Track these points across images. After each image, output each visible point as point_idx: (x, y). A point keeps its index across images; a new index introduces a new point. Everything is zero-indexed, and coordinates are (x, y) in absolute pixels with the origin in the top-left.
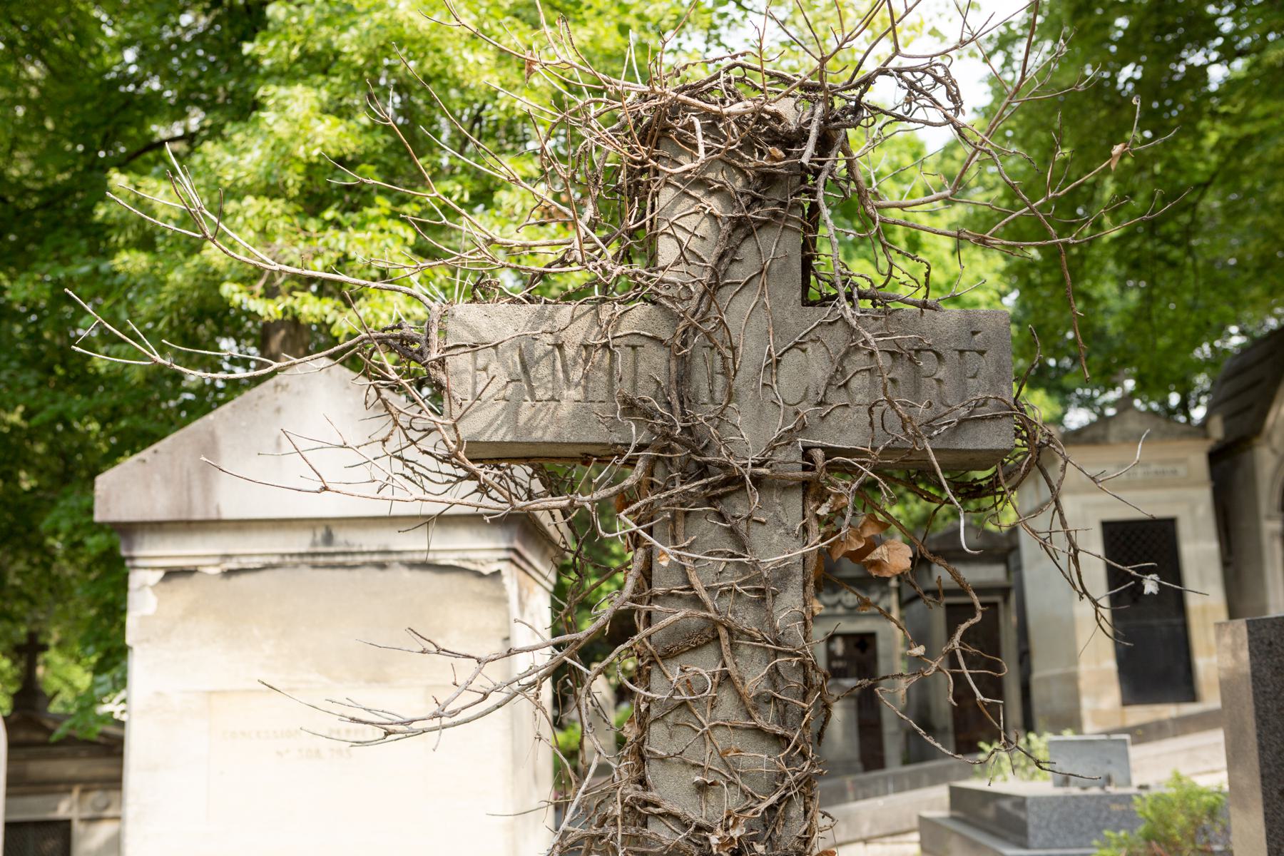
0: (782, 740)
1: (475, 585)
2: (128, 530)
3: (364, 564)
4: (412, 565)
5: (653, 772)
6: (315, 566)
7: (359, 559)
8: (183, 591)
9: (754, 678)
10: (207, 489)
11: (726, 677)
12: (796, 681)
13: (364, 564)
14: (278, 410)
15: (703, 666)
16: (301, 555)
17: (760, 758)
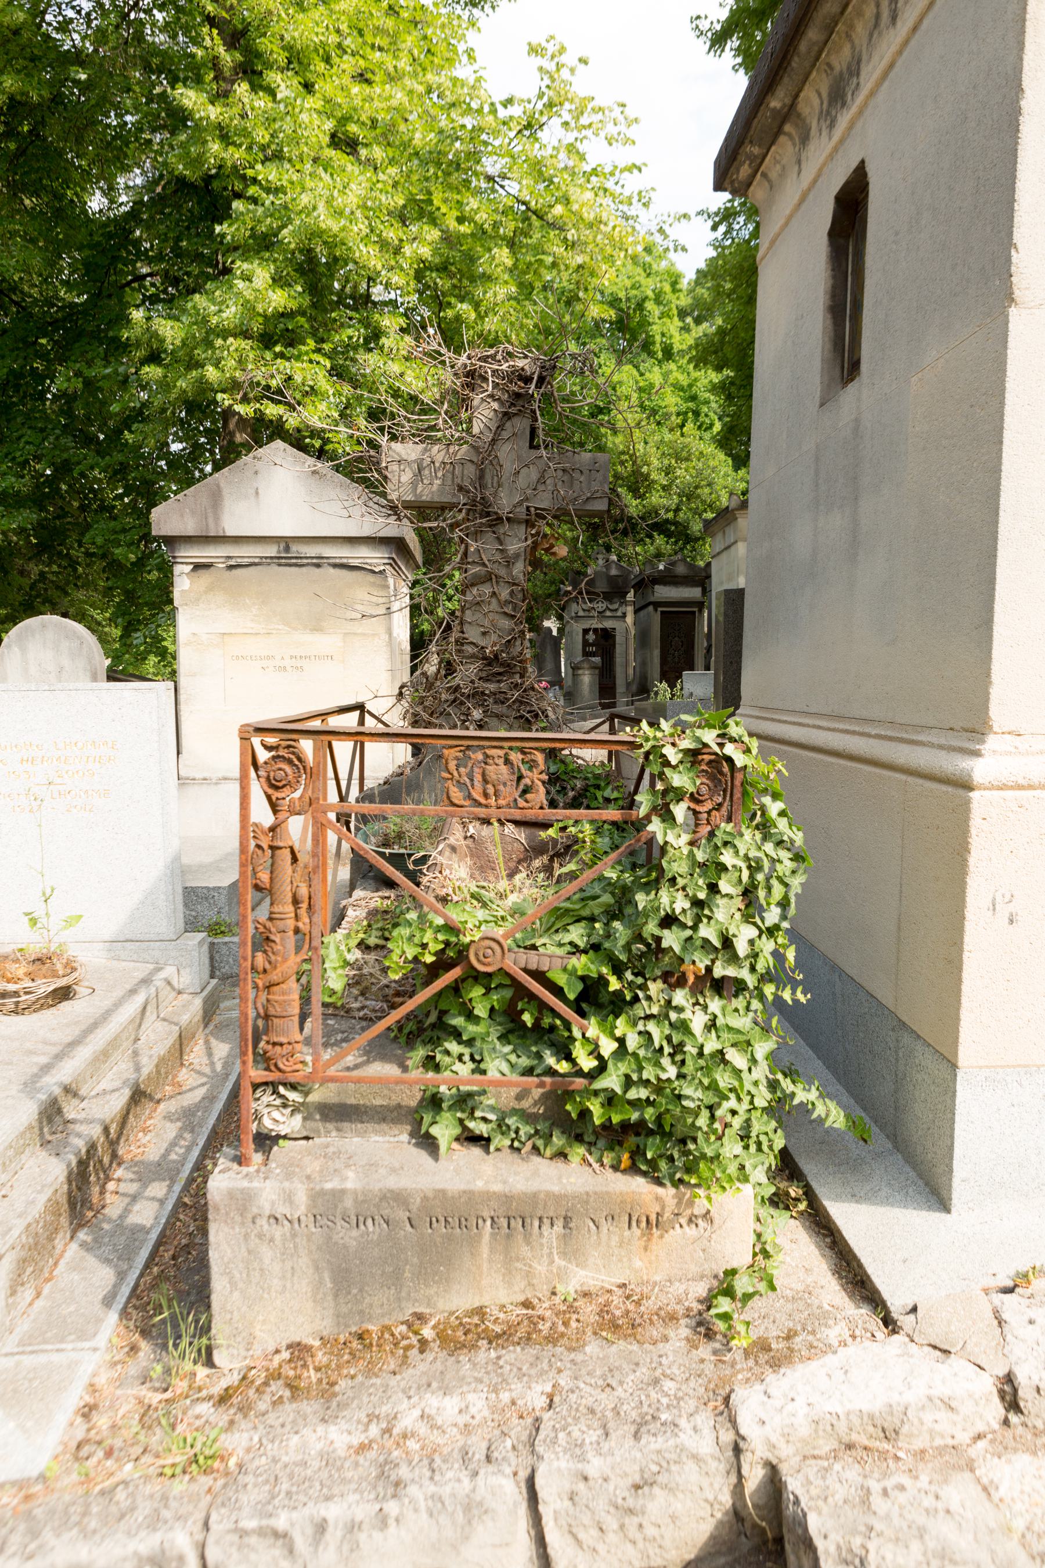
0: (513, 617)
1: (371, 578)
2: (172, 541)
3: (308, 564)
4: (335, 566)
5: (466, 628)
6: (280, 565)
7: (305, 561)
8: (205, 576)
9: (504, 593)
10: (217, 519)
11: (494, 593)
12: (520, 596)
13: (308, 564)
14: (256, 473)
15: (487, 589)
16: (271, 558)
17: (506, 623)
